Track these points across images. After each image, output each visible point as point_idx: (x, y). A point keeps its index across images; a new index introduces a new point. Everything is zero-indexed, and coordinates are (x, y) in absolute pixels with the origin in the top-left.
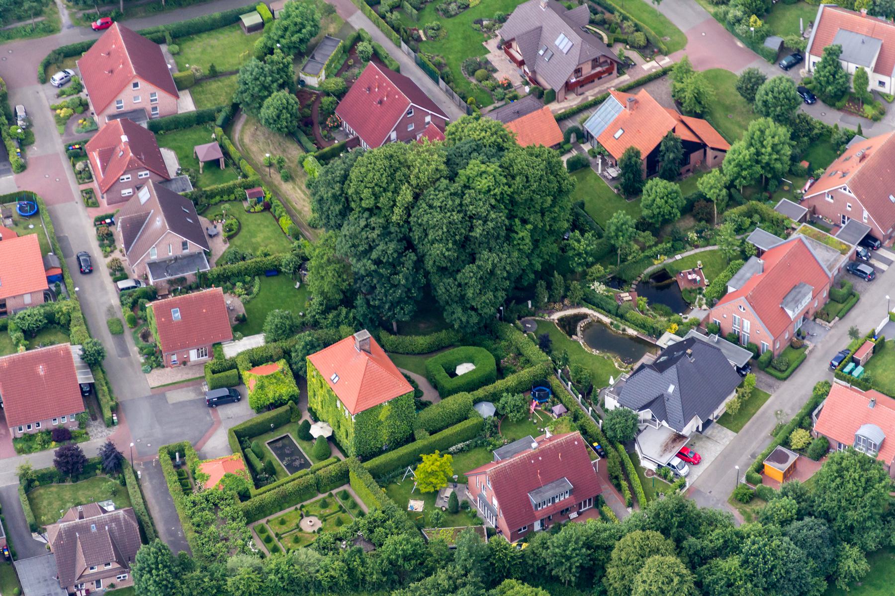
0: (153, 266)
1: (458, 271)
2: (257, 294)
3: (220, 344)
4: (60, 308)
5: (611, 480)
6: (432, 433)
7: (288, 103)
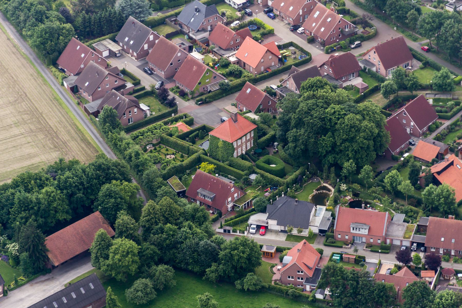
6: (230, 165)
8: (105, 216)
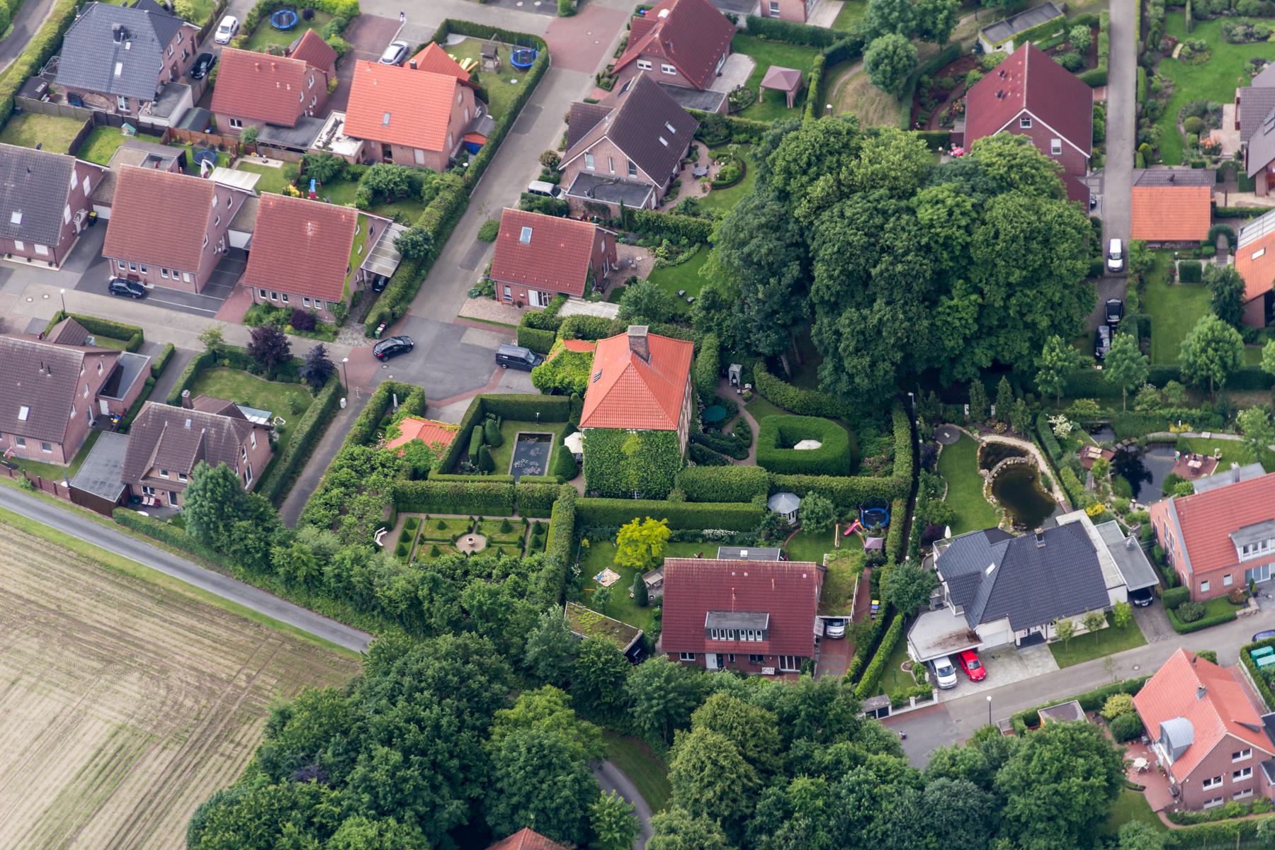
6: (689, 499)
7: (894, 52)
8: (552, 832)
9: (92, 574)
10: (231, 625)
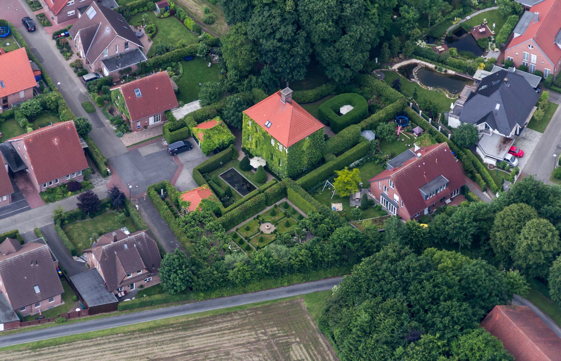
0: (106, 61)
1: (335, 42)
2: (183, 74)
3: (169, 111)
4: (49, 98)
5: (466, 175)
6: (337, 155)
9: (141, 337)
10: (225, 319)
